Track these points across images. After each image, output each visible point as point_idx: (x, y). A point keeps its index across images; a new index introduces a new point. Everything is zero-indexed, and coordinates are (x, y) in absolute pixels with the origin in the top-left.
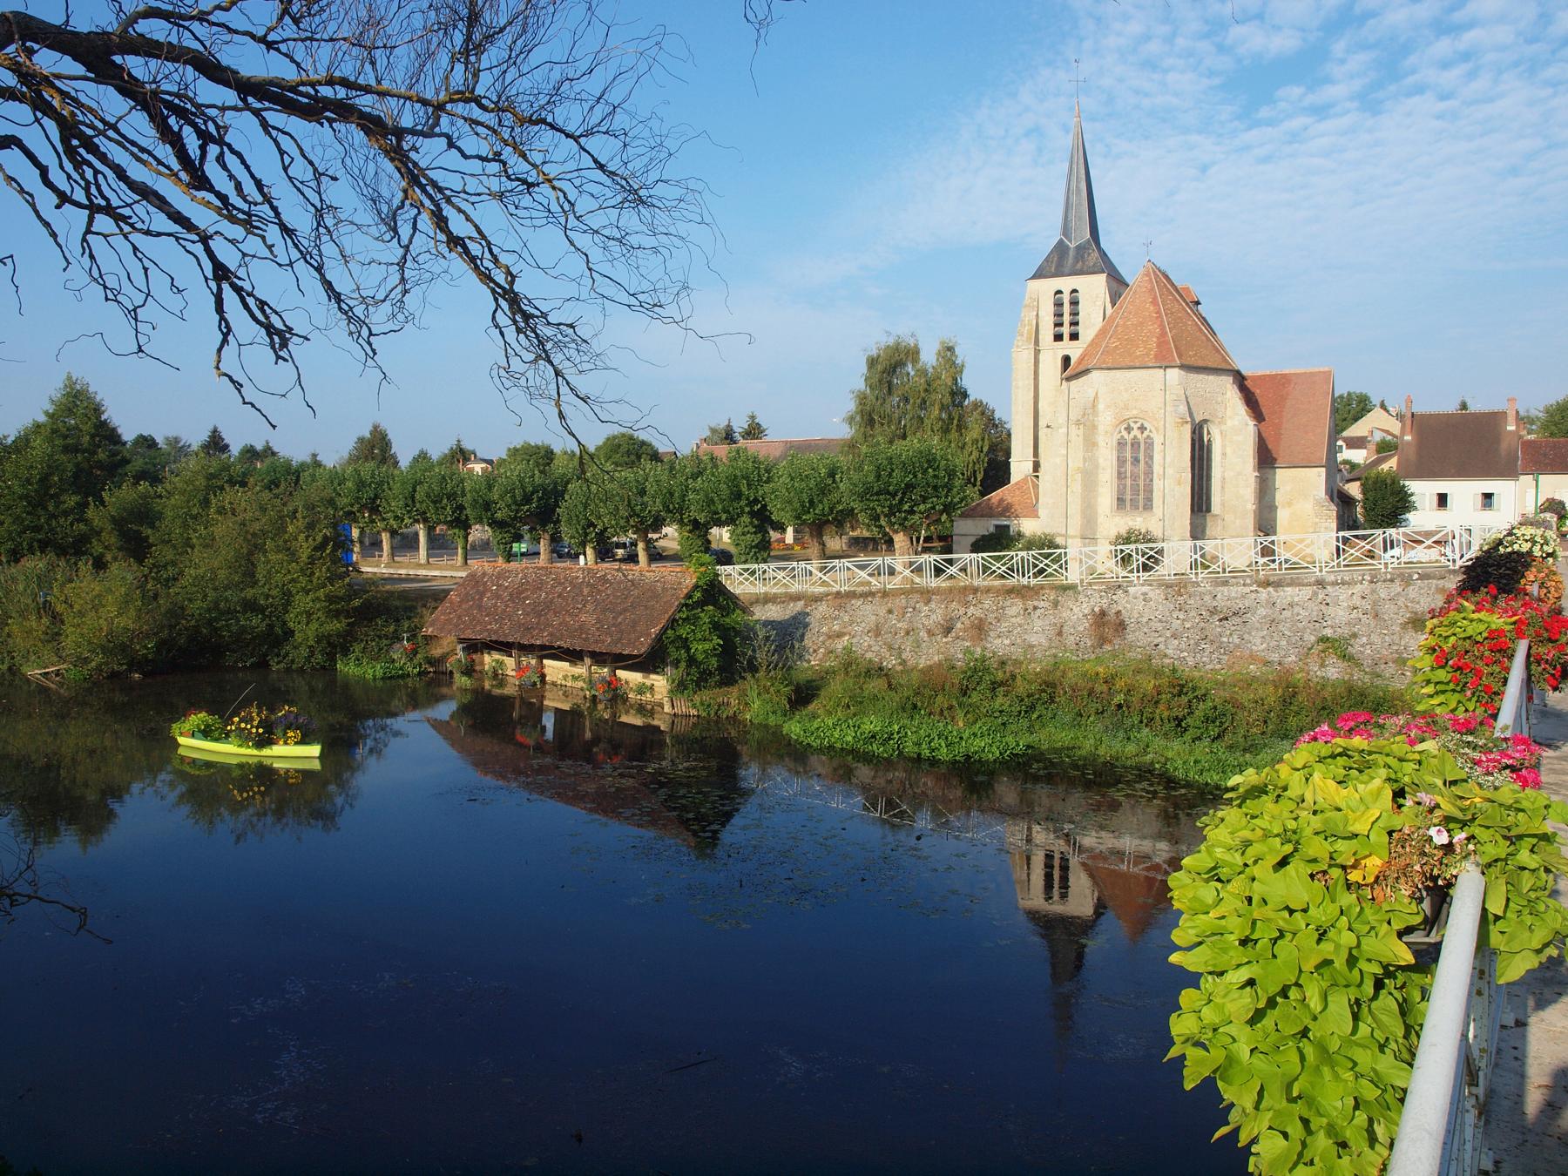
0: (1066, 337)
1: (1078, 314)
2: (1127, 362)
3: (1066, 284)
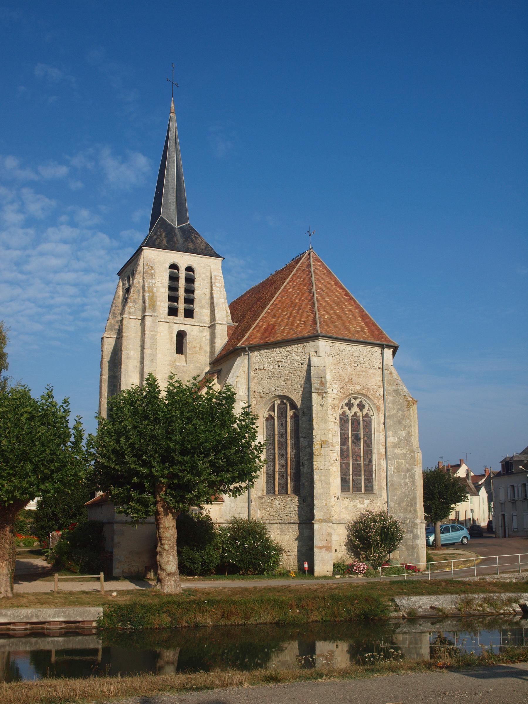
0: (181, 312)
1: (192, 292)
2: (341, 333)
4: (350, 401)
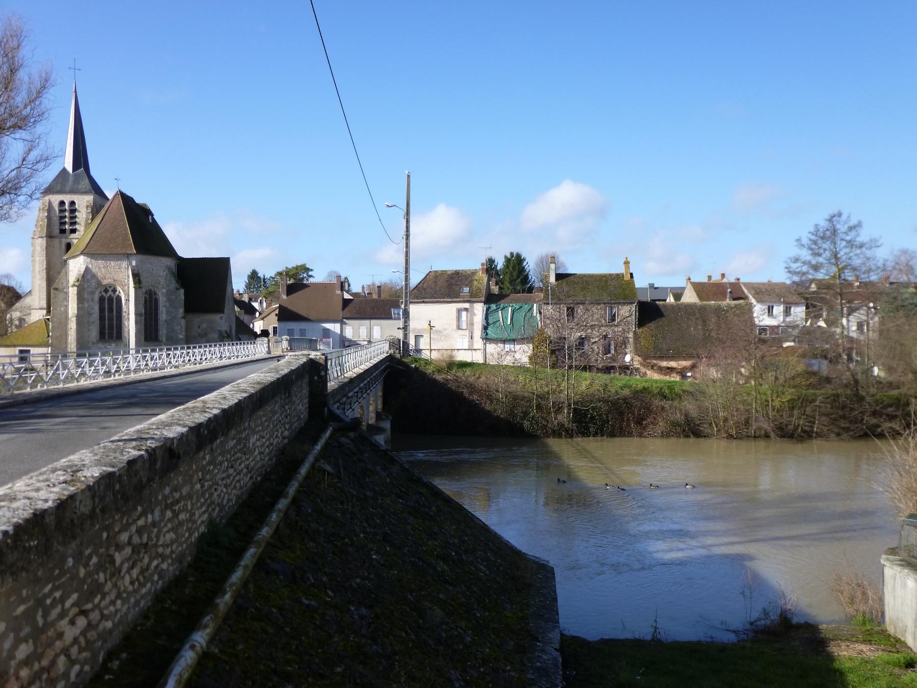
3: (67, 198)
4: (106, 289)
